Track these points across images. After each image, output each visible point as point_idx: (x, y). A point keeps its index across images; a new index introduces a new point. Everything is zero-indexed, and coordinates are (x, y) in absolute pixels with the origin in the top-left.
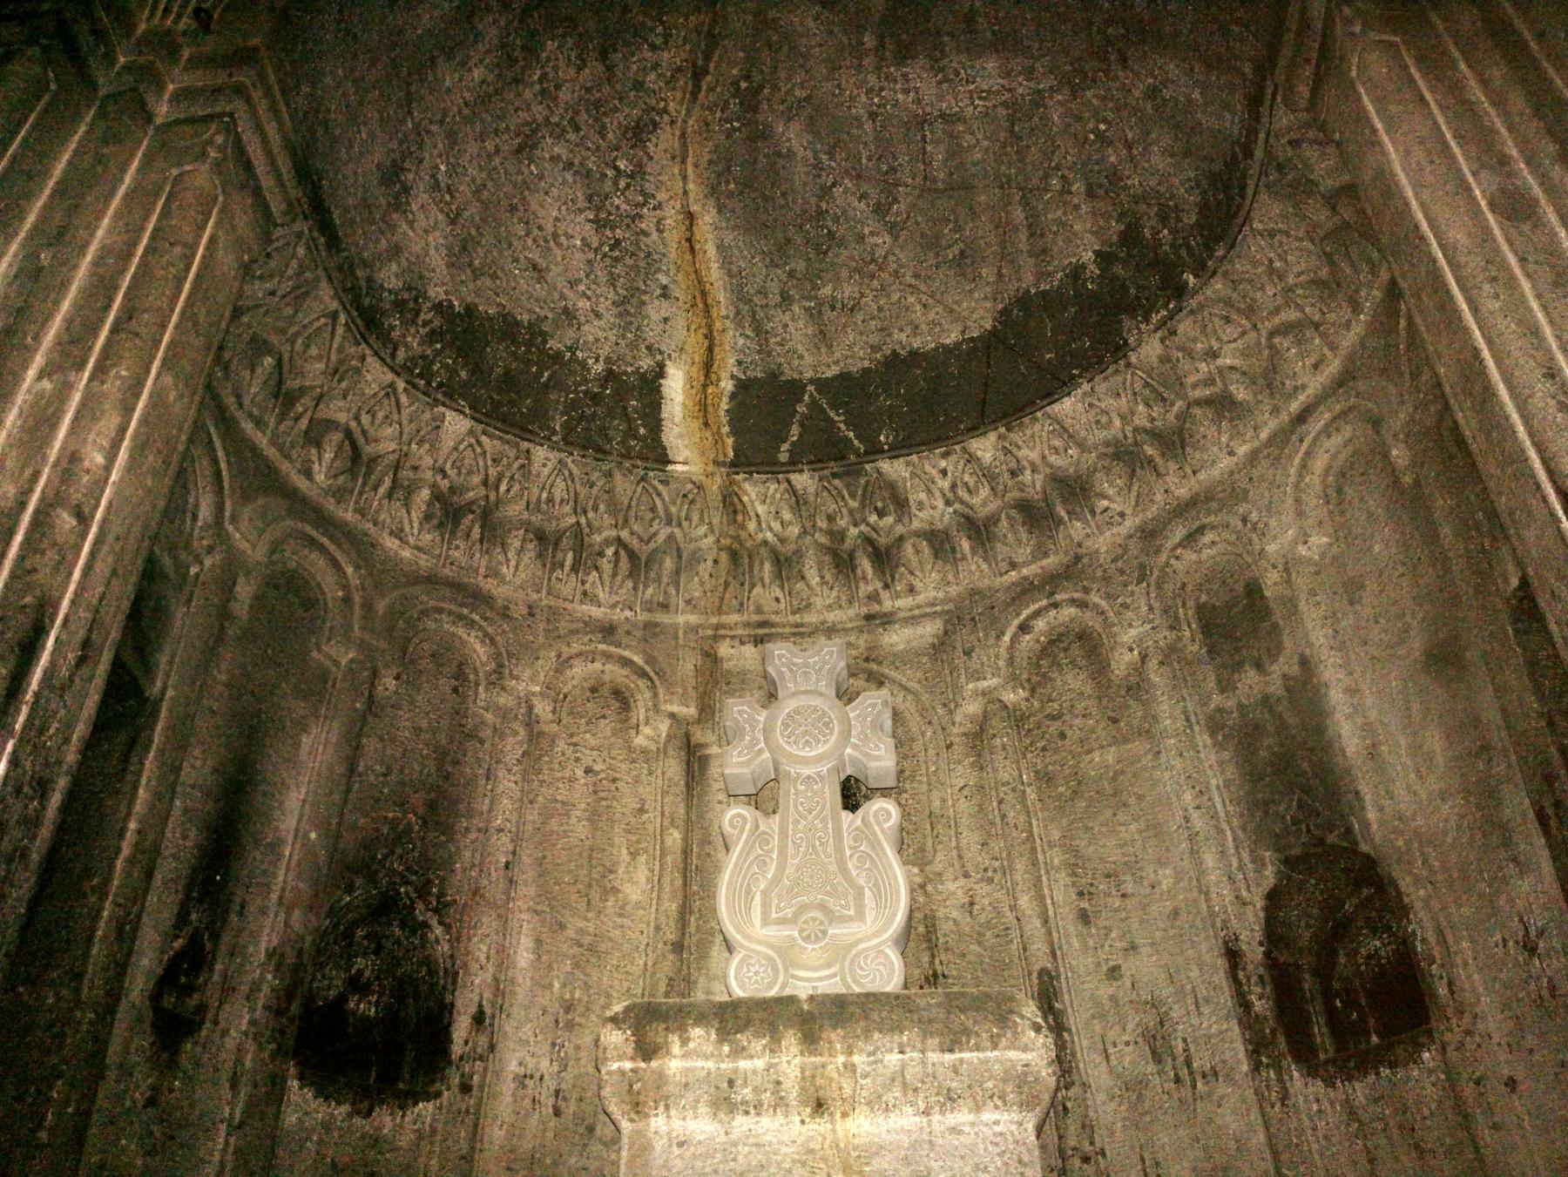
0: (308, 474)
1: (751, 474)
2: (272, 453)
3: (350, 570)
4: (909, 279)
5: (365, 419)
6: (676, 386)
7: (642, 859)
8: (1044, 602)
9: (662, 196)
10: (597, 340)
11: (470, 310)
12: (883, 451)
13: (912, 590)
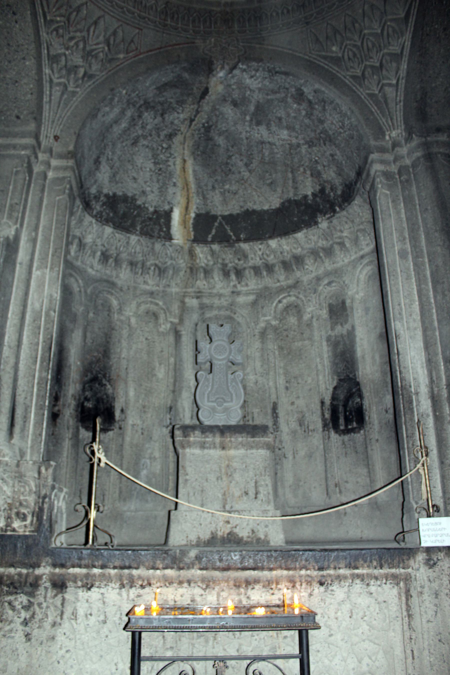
3: (80, 281)
4: (254, 187)
5: (84, 233)
6: (176, 216)
7: (163, 366)
8: (286, 294)
9: (176, 155)
11: (115, 194)
13: (247, 285)
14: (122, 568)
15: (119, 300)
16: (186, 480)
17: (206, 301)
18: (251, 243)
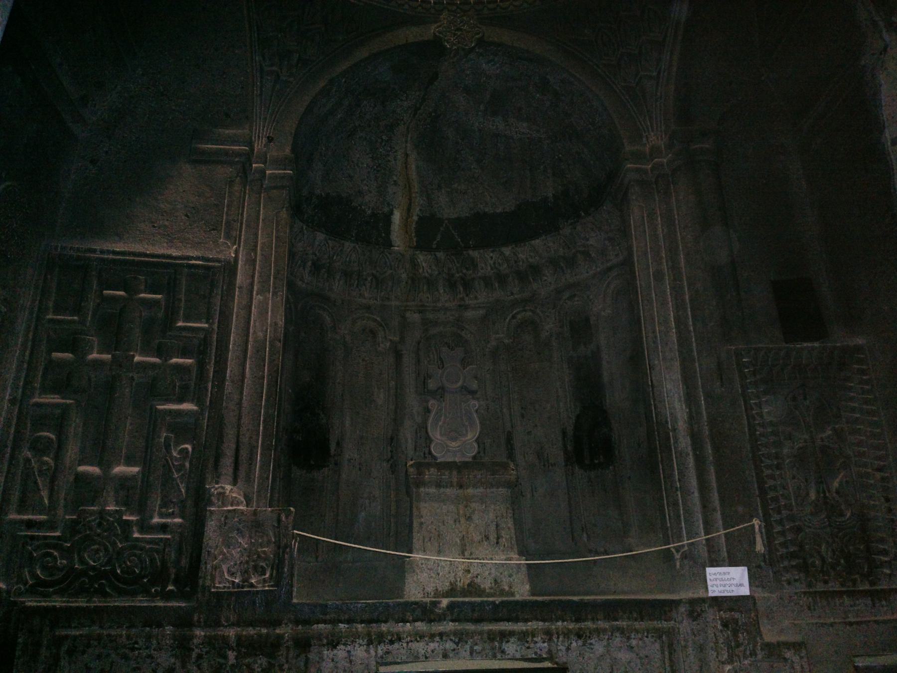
5: (293, 241)
6: (397, 217)
12: (469, 248)
13: (476, 298)
14: (369, 622)
16: (422, 523)
17: (430, 316)
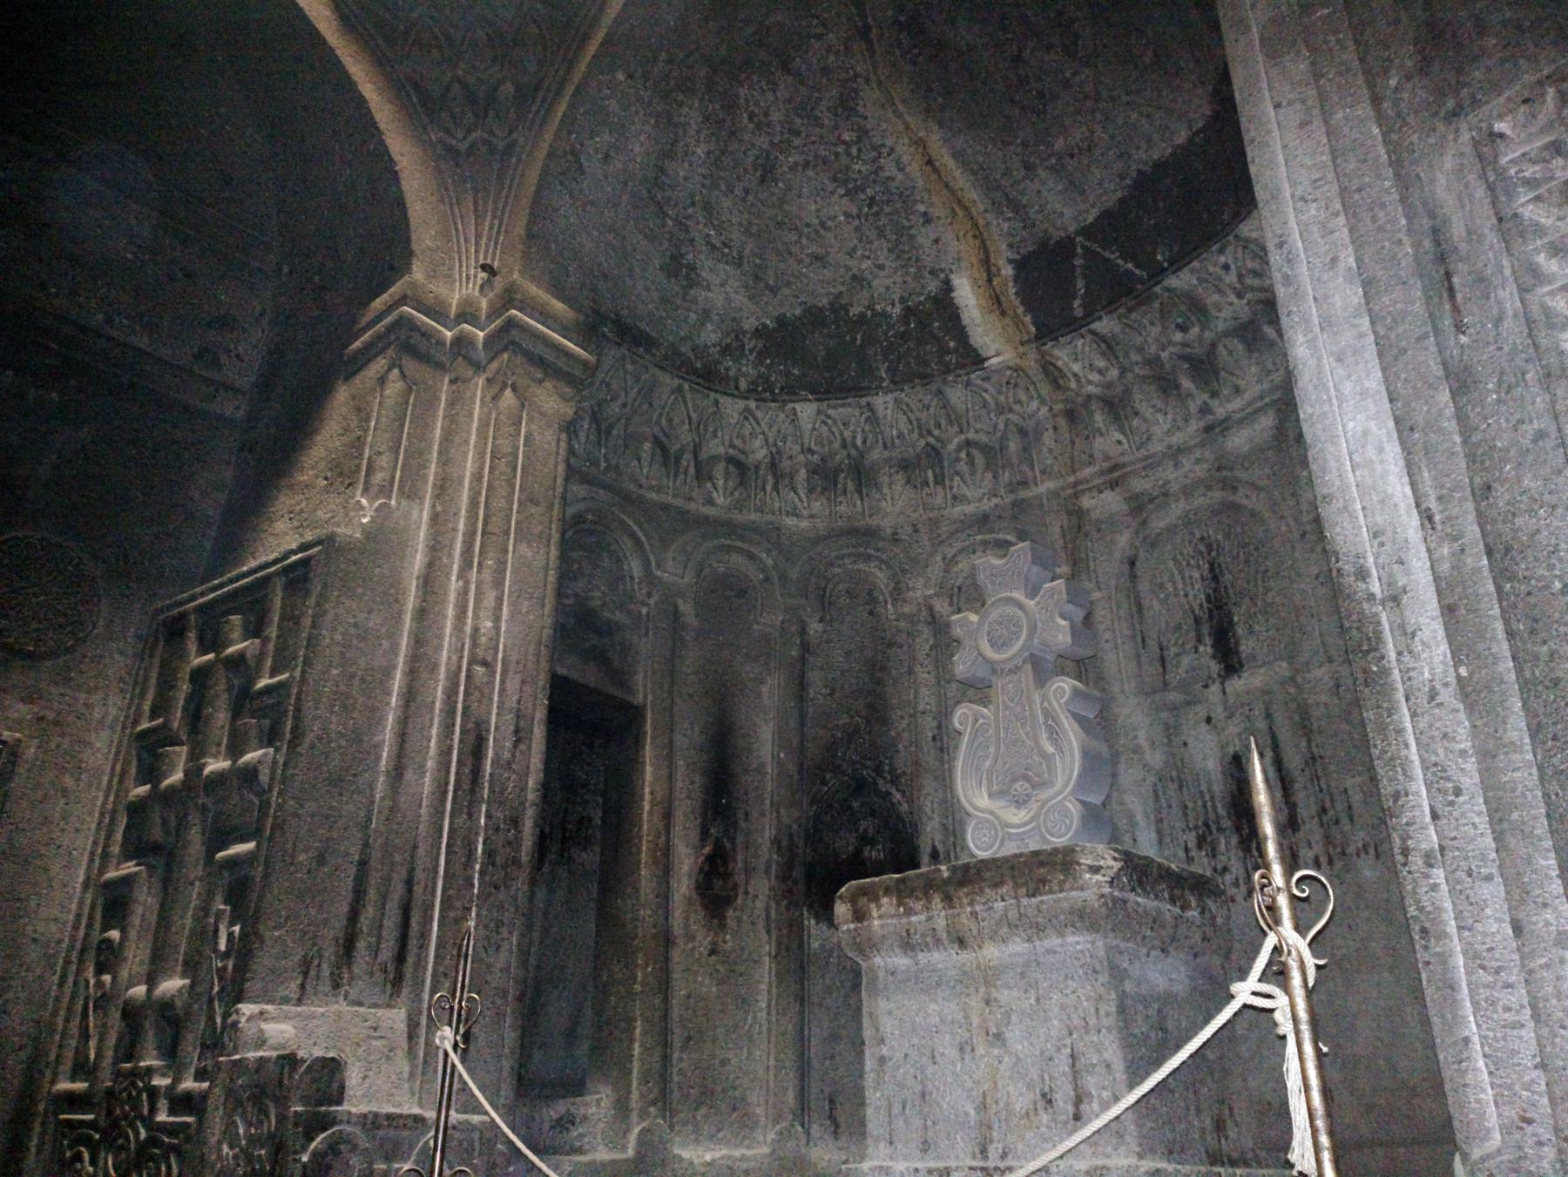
0: (710, 502)
1: (1056, 339)
2: (679, 502)
4: (1124, 98)
5: (737, 442)
6: (966, 294)
9: (889, 142)
10: (888, 288)
12: (1164, 270)
13: (1237, 391)
15: (889, 567)
16: (882, 1060)
17: (1138, 485)
18: (1195, 264)
